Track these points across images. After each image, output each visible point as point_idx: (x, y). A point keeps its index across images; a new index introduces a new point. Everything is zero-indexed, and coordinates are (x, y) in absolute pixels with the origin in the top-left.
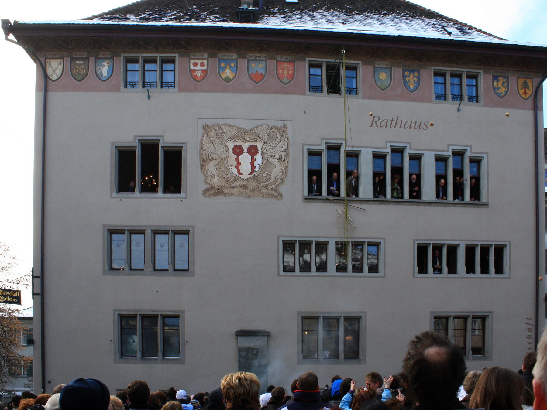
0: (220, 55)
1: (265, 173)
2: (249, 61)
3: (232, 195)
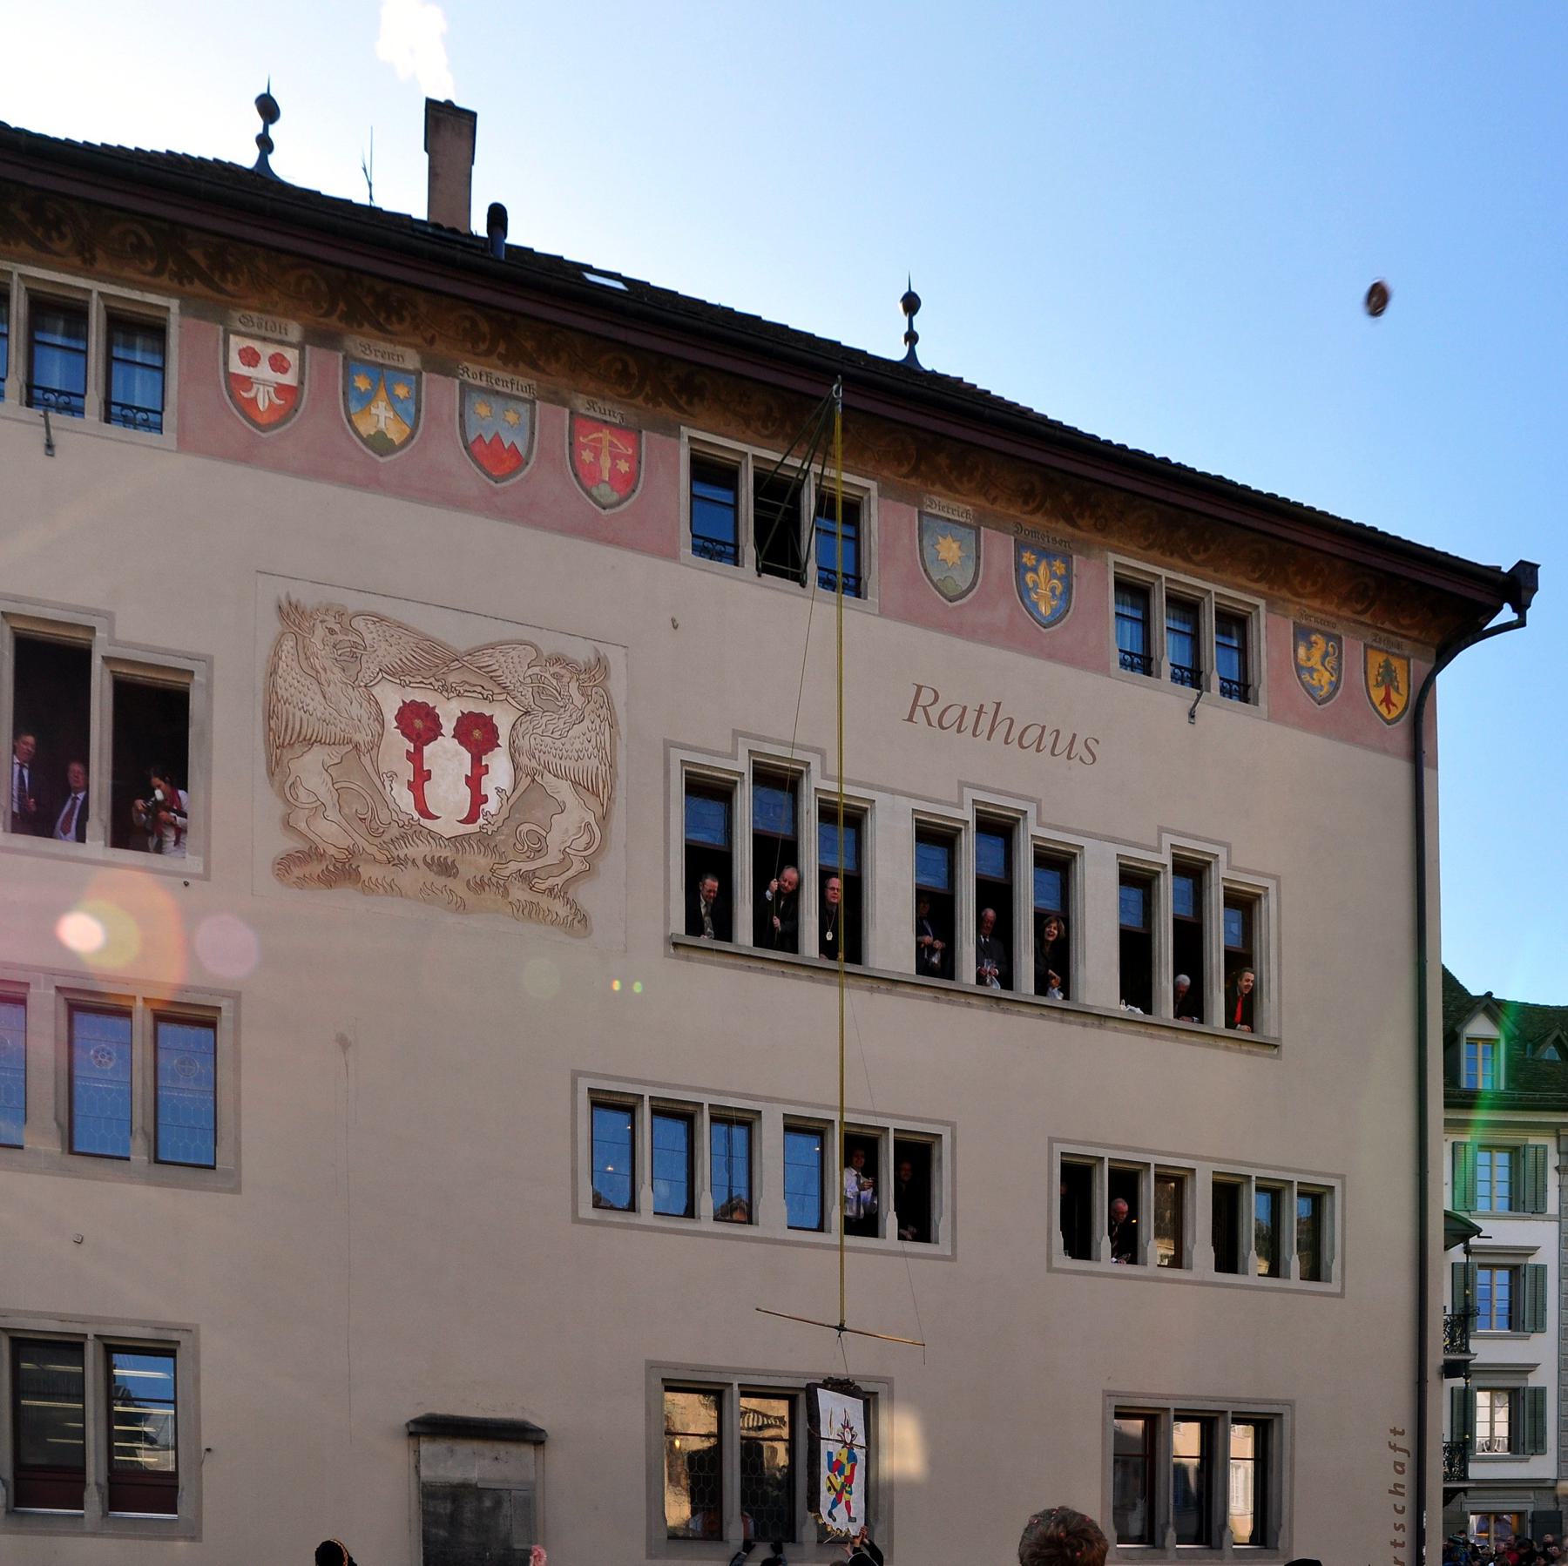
0: (356, 343)
1: (525, 828)
2: (465, 389)
3: (392, 889)
